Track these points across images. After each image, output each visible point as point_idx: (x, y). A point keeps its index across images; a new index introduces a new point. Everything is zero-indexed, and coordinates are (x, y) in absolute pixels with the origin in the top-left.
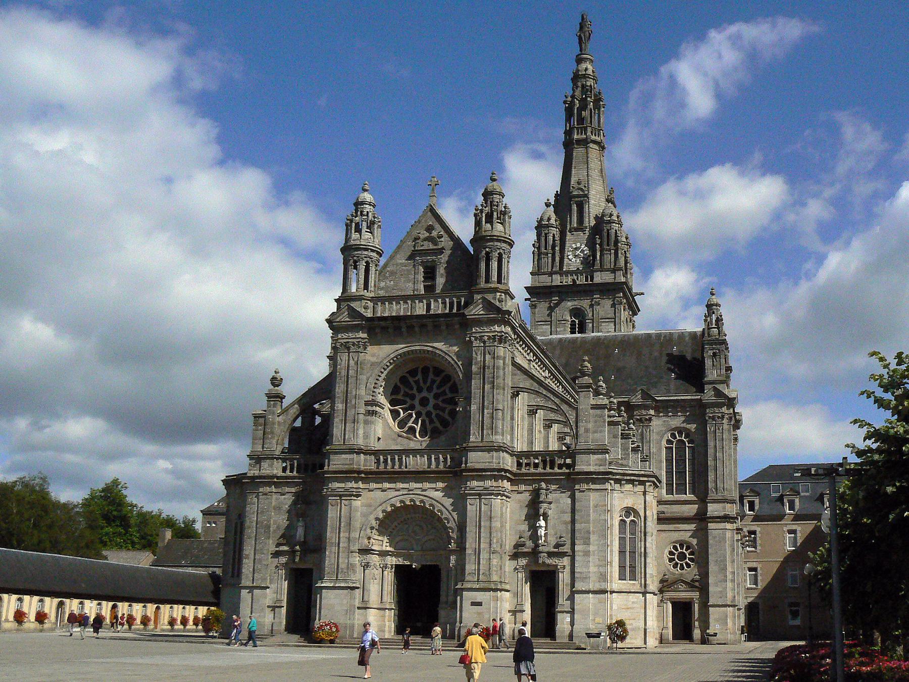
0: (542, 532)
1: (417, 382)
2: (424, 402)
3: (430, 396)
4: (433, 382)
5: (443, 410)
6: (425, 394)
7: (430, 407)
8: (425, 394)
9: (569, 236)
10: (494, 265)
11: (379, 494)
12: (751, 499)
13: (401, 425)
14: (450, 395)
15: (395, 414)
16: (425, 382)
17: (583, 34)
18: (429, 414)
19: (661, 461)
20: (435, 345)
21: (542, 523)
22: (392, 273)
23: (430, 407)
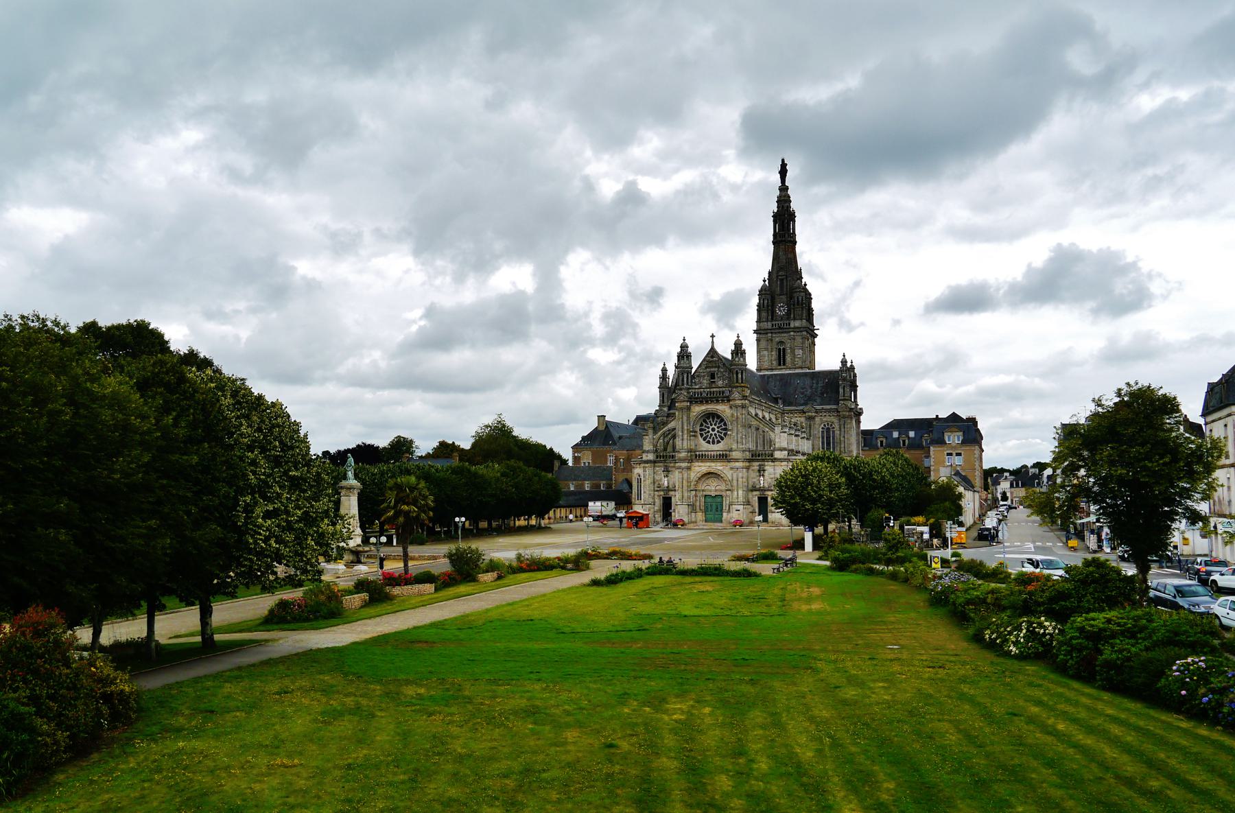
0: (762, 482)
1: (710, 422)
2: (713, 430)
3: (716, 427)
4: (717, 421)
5: (721, 433)
6: (713, 426)
7: (716, 432)
8: (713, 426)
9: (777, 299)
10: (740, 376)
11: (696, 468)
12: (881, 439)
13: (704, 439)
14: (724, 427)
15: (702, 435)
16: (713, 421)
17: (783, 172)
18: (715, 435)
19: (819, 438)
20: (717, 407)
21: (762, 478)
22: (698, 376)
23: (716, 432)
